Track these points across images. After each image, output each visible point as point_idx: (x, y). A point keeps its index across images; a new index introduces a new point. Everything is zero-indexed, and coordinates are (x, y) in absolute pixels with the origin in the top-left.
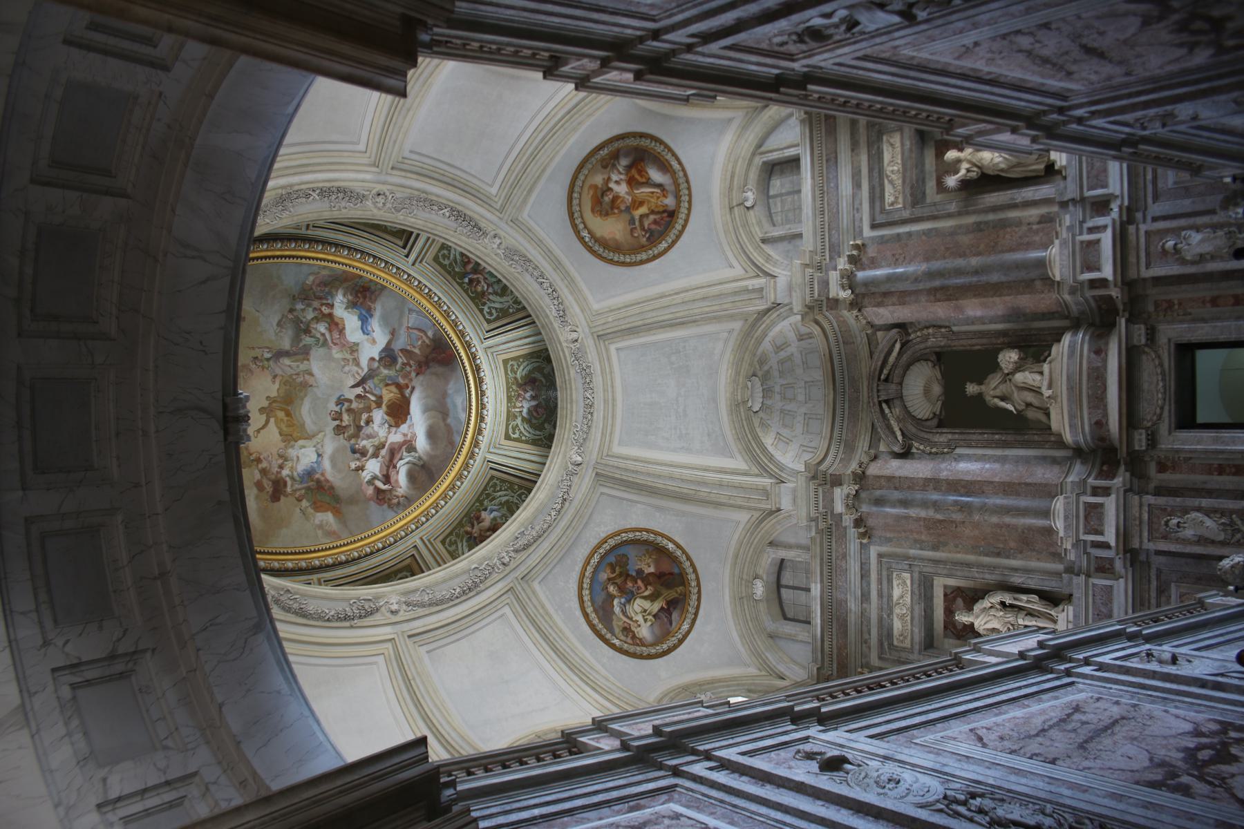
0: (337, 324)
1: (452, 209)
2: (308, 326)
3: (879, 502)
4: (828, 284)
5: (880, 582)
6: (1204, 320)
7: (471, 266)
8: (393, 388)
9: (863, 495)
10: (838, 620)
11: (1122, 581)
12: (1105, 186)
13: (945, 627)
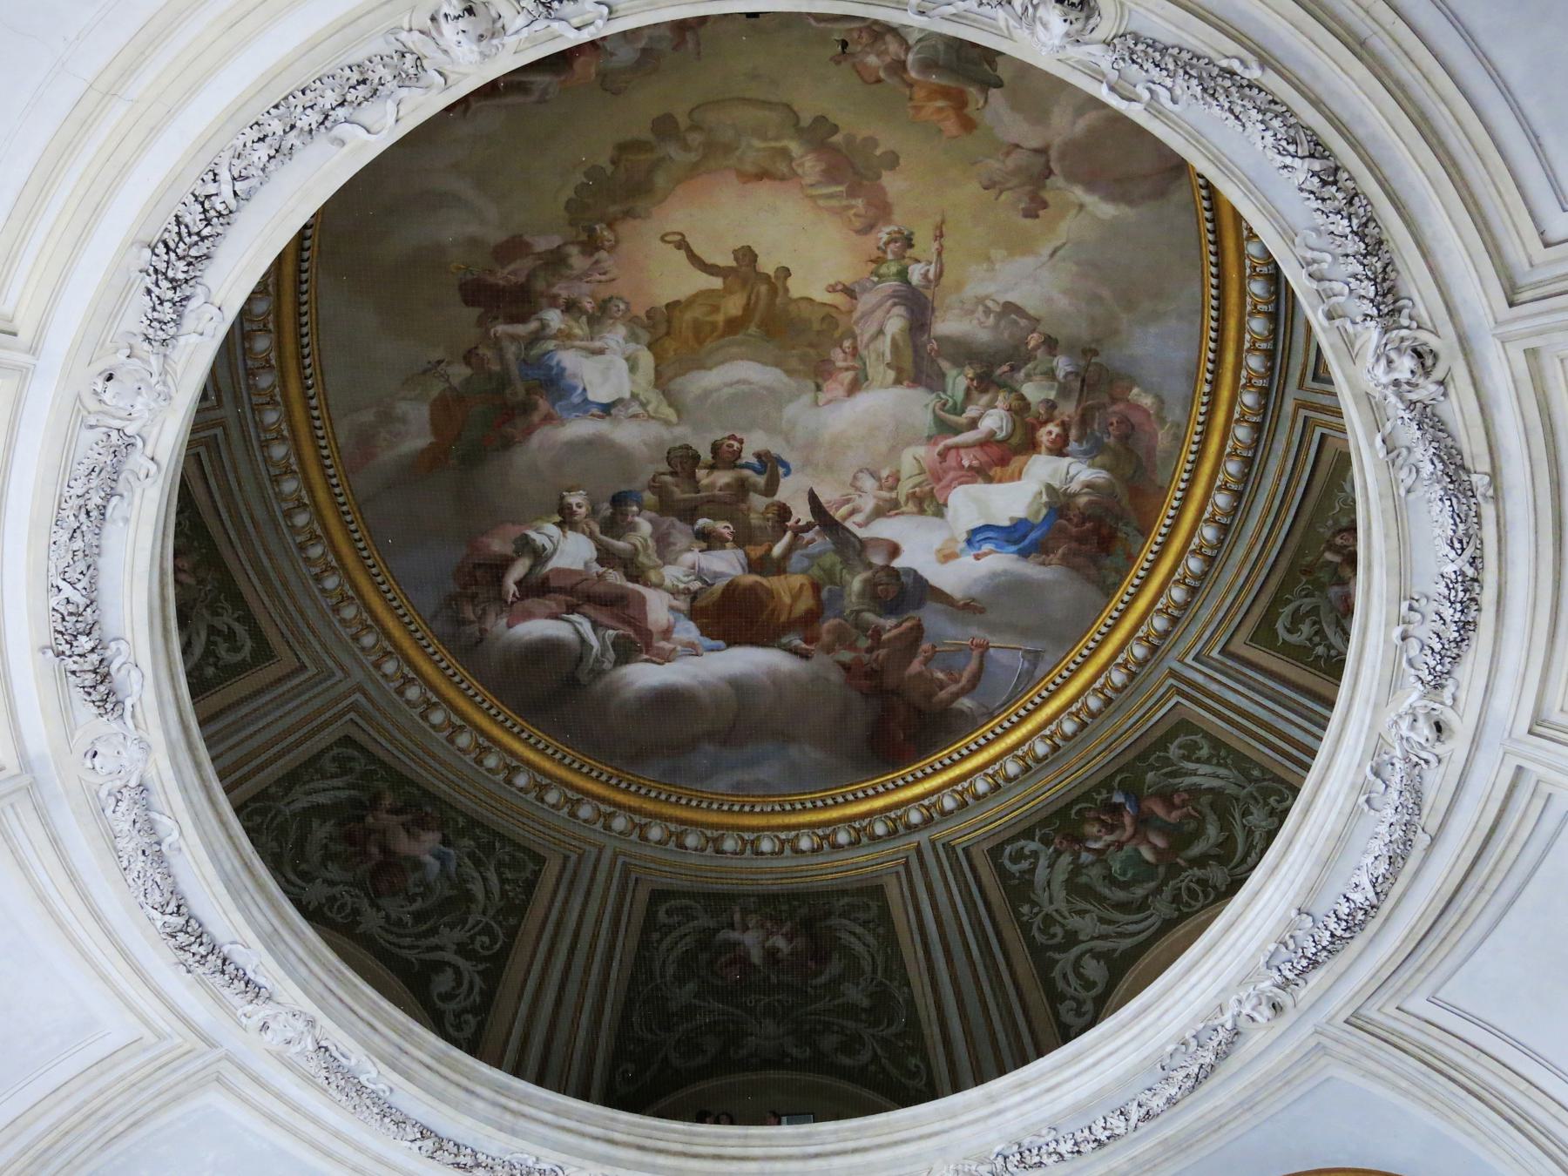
0: (1003, 462)
1: (1371, 910)
2: (1001, 386)
7: (1159, 810)
8: (805, 603)
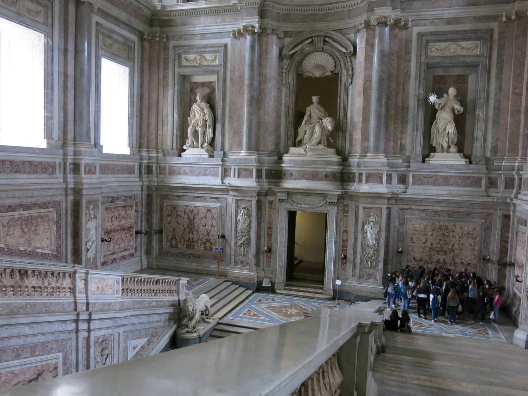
4: (384, 6)
5: (212, 46)
6: (337, 227)
11: (220, 182)
12: (413, 183)
13: (195, 83)
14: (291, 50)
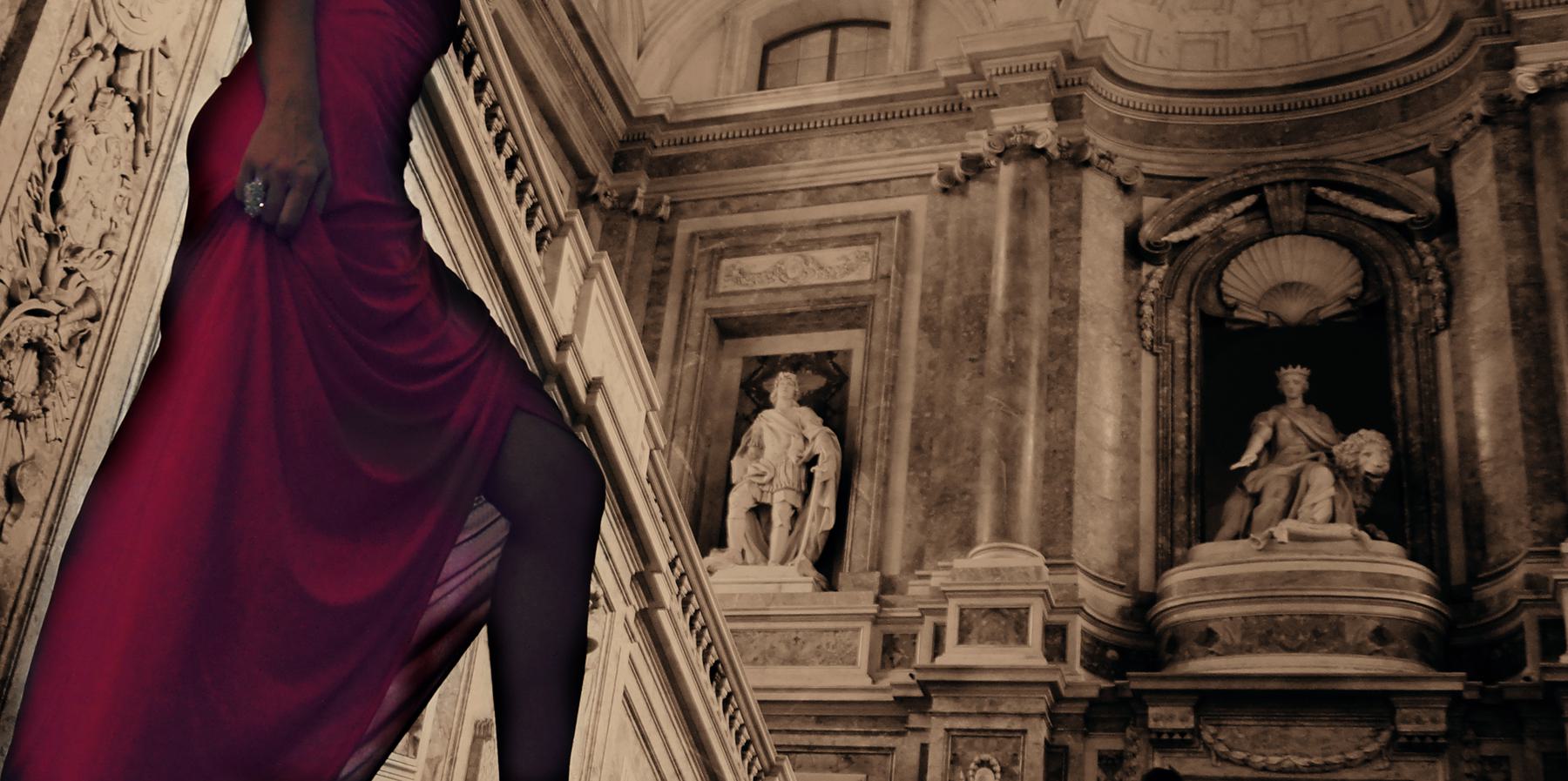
3: (1022, 197)
9: (1036, 166)
10: (768, 146)
13: (764, 359)
14: (1175, 229)
